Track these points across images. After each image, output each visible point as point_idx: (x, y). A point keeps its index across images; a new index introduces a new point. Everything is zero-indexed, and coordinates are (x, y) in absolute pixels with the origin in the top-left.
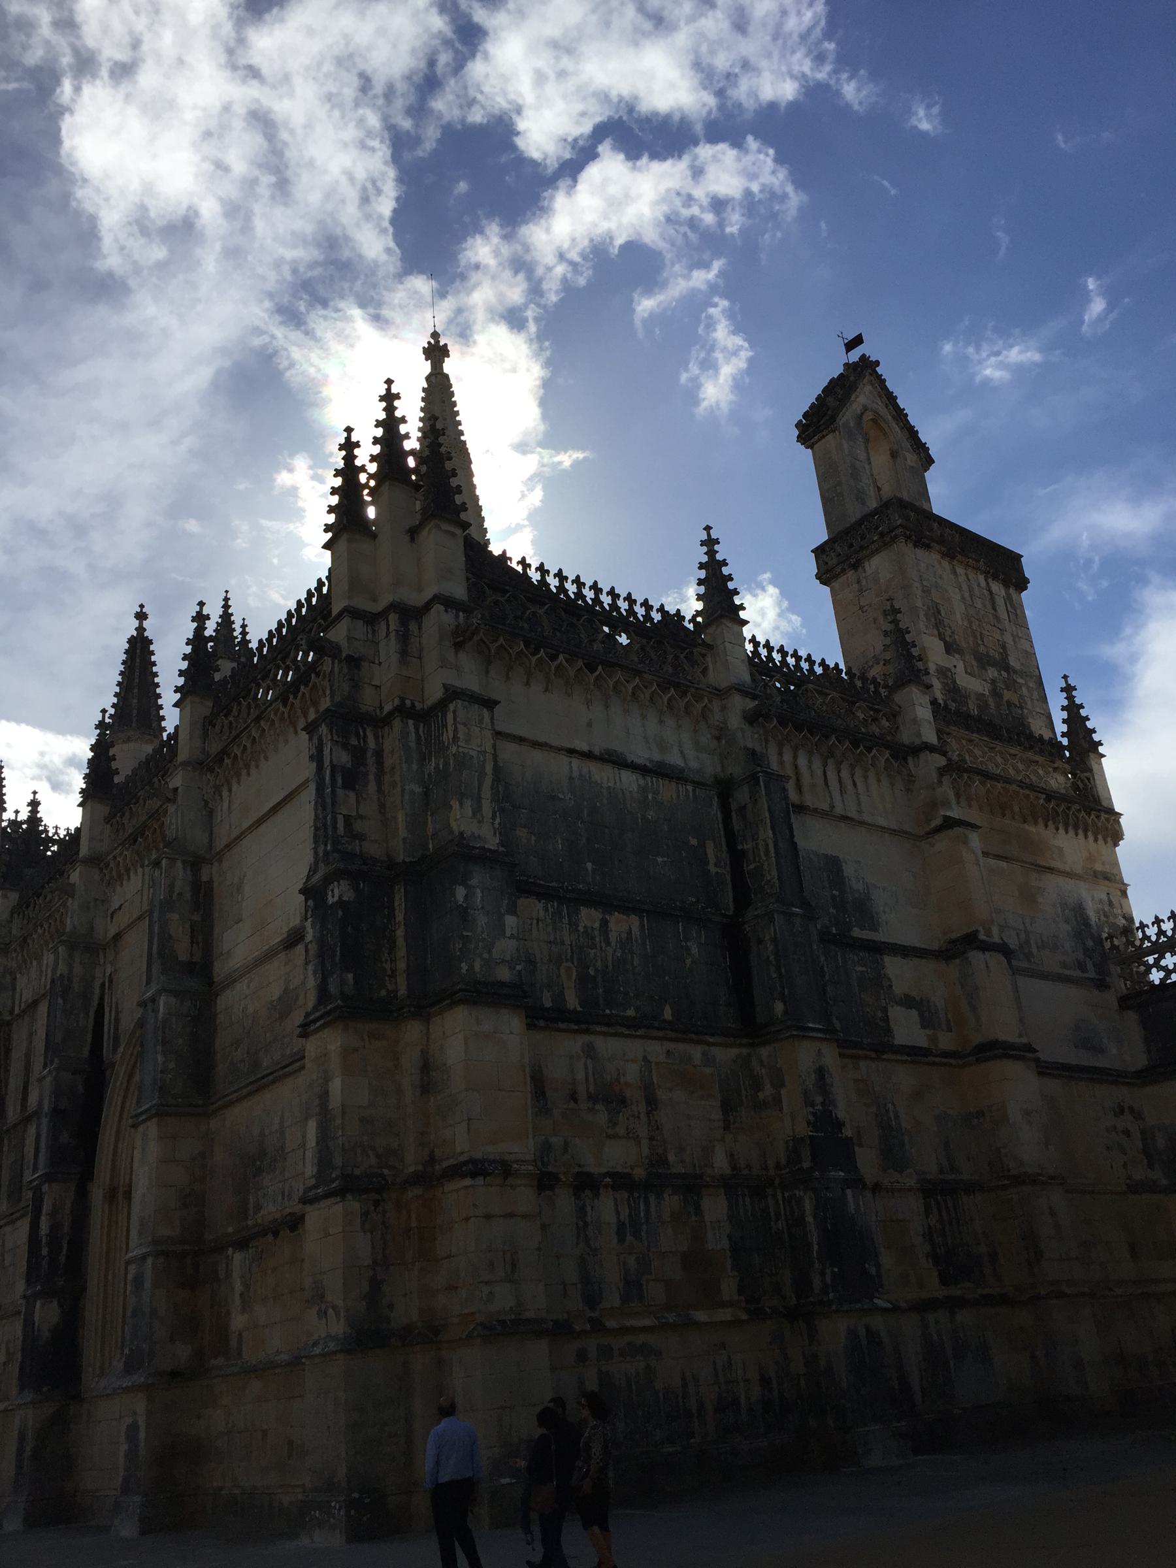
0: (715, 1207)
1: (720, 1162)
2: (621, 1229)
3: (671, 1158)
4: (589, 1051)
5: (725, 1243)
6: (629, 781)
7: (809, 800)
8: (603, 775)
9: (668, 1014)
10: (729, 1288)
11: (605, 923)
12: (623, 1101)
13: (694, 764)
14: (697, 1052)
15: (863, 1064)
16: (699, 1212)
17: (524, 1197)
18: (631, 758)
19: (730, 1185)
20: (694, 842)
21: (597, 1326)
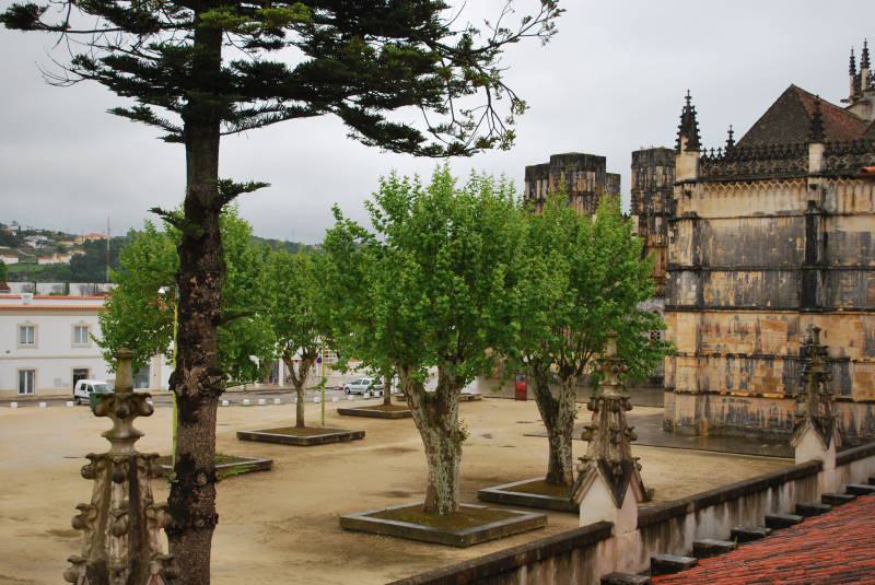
0: (779, 366)
1: (783, 351)
2: (741, 370)
3: (763, 350)
4: (737, 318)
5: (781, 376)
6: (765, 222)
7: (858, 209)
8: (754, 223)
9: (769, 304)
10: (780, 388)
11: (747, 276)
12: (747, 333)
13: (797, 208)
14: (779, 317)
15: (862, 317)
16: (772, 366)
17: (692, 362)
18: (767, 213)
19: (784, 358)
20: (791, 240)
21: (728, 394)
